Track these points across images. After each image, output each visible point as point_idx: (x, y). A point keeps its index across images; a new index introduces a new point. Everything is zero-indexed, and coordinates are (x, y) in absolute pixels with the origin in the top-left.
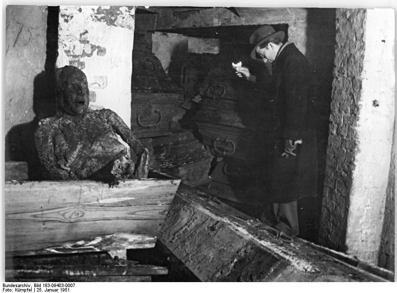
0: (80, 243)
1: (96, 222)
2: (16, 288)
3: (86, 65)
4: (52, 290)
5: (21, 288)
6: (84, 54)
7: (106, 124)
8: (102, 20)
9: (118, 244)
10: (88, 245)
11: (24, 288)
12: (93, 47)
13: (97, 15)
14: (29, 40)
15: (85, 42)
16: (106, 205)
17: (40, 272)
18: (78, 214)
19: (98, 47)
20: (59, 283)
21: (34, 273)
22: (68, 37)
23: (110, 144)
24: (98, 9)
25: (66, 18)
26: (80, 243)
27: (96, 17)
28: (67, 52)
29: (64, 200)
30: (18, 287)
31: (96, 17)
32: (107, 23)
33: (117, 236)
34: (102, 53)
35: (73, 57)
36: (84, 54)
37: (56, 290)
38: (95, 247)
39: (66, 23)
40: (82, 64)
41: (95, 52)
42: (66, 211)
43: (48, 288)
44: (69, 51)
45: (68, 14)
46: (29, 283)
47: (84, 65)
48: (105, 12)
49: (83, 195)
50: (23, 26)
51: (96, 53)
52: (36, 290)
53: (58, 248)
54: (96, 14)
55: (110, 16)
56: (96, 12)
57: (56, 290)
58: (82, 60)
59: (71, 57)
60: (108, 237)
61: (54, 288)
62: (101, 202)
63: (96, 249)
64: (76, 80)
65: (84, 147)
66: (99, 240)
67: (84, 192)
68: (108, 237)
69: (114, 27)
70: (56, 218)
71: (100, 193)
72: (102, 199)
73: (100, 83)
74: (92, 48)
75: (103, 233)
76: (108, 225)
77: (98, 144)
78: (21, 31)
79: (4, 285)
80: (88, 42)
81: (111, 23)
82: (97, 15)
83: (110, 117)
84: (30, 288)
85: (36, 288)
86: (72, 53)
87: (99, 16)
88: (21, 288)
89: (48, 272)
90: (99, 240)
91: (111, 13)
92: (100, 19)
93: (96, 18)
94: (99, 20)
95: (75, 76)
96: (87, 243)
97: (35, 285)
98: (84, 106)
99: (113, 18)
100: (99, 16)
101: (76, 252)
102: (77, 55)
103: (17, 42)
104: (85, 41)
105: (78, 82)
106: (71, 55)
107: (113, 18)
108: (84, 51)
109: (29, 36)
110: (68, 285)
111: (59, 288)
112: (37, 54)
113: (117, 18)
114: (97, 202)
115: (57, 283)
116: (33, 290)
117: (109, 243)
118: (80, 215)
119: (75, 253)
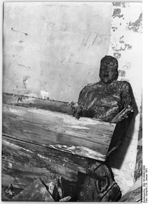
0: (65, 146)
1: (72, 137)
3: (121, 55)
6: (121, 49)
7: (119, 89)
8: (131, 29)
9: (83, 153)
10: (69, 149)
12: (126, 45)
13: (129, 27)
14: (101, 41)
15: (122, 42)
16: (75, 129)
17: (28, 151)
18: (62, 131)
19: (128, 45)
21: (26, 151)
22: (114, 40)
23: (110, 100)
24: (130, 23)
25: (114, 29)
26: (65, 146)
27: (128, 27)
28: (113, 48)
29: (55, 121)
31: (128, 27)
32: (134, 31)
33: (83, 148)
34: (130, 49)
35: (116, 51)
36: (121, 49)
38: (72, 151)
39: (114, 32)
40: (120, 55)
41: (127, 48)
42: (57, 128)
44: (114, 48)
45: (115, 27)
47: (121, 55)
48: (133, 24)
49: (63, 121)
50: (98, 34)
51: (127, 48)
53: (55, 146)
54: (129, 26)
55: (135, 27)
56: (129, 25)
58: (120, 52)
59: (115, 51)
60: (78, 147)
62: (73, 127)
63: (73, 152)
64: (105, 64)
65: (97, 100)
66: (73, 148)
67: (64, 119)
68: (78, 147)
69: (137, 33)
70: (53, 130)
71: (71, 121)
72: (72, 125)
73: (128, 66)
74: (125, 45)
75: (75, 145)
76: (77, 141)
77: (105, 99)
78: (97, 37)
80: (123, 42)
81: (136, 30)
82: (129, 27)
83: (123, 86)
86: (115, 49)
87: (130, 27)
89: (32, 152)
90: (73, 148)
91: (136, 24)
92: (130, 29)
93: (128, 28)
94: (130, 29)
95: (105, 61)
96: (68, 148)
98: (109, 78)
99: (137, 28)
100: (130, 27)
101: (64, 151)
102: (118, 50)
103: (95, 43)
104: (122, 42)
105: (106, 64)
106: (115, 50)
107: (137, 28)
108: (121, 47)
109: (101, 39)
112: (104, 49)
113: (139, 27)
114: (70, 126)
117: (79, 151)
118: (63, 131)
119: (63, 152)
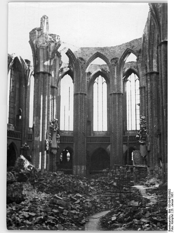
2: (171, 223)
4: (172, 203)
5: (171, 220)
11: (171, 219)
20: (168, 198)
30: (171, 223)
37: (172, 200)
43: (171, 205)
46: (168, 216)
52: (172, 212)
57: (172, 200)
61: (171, 201)
79: (169, 231)
84: (171, 216)
85: (171, 212)
88: (171, 220)
97: (170, 212)
110: (169, 193)
111: (171, 198)
115: (168, 200)
116: (172, 214)
